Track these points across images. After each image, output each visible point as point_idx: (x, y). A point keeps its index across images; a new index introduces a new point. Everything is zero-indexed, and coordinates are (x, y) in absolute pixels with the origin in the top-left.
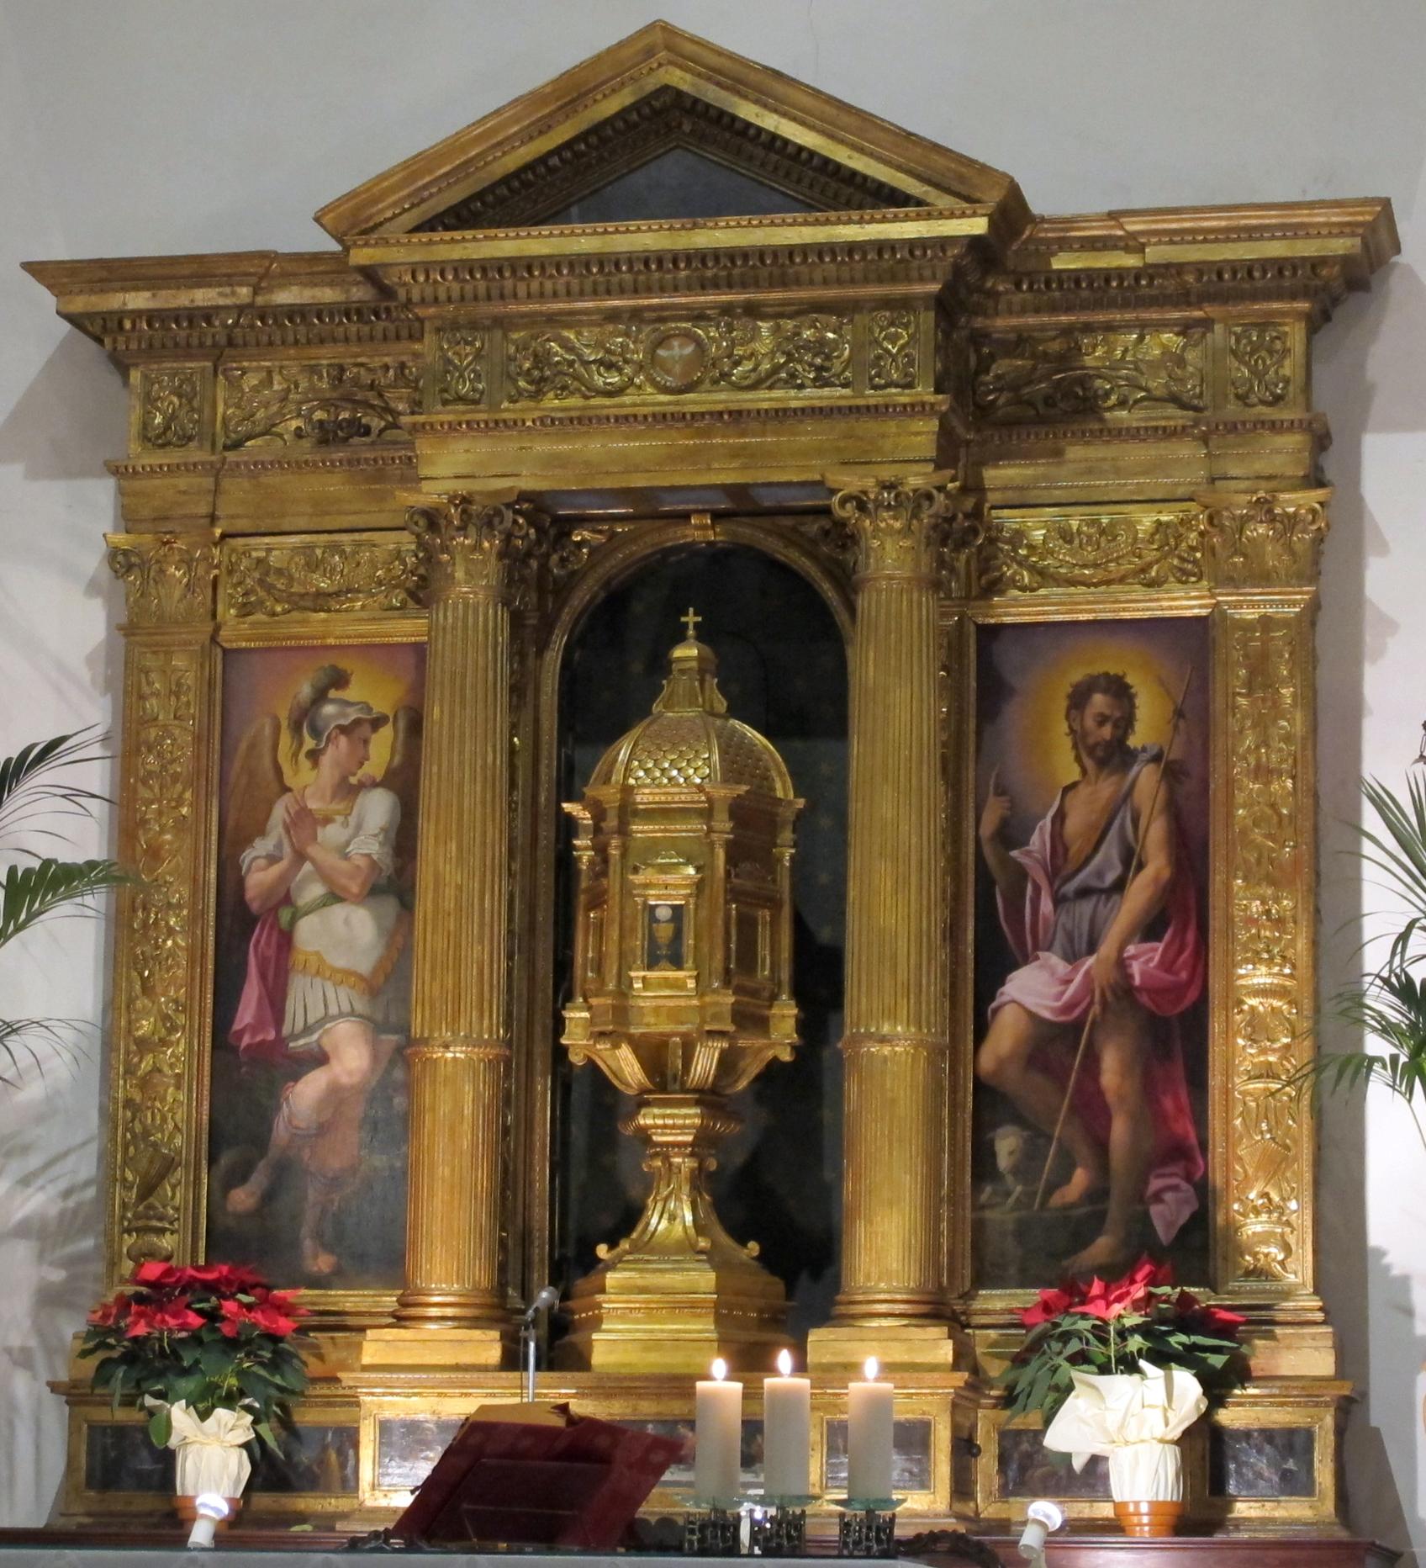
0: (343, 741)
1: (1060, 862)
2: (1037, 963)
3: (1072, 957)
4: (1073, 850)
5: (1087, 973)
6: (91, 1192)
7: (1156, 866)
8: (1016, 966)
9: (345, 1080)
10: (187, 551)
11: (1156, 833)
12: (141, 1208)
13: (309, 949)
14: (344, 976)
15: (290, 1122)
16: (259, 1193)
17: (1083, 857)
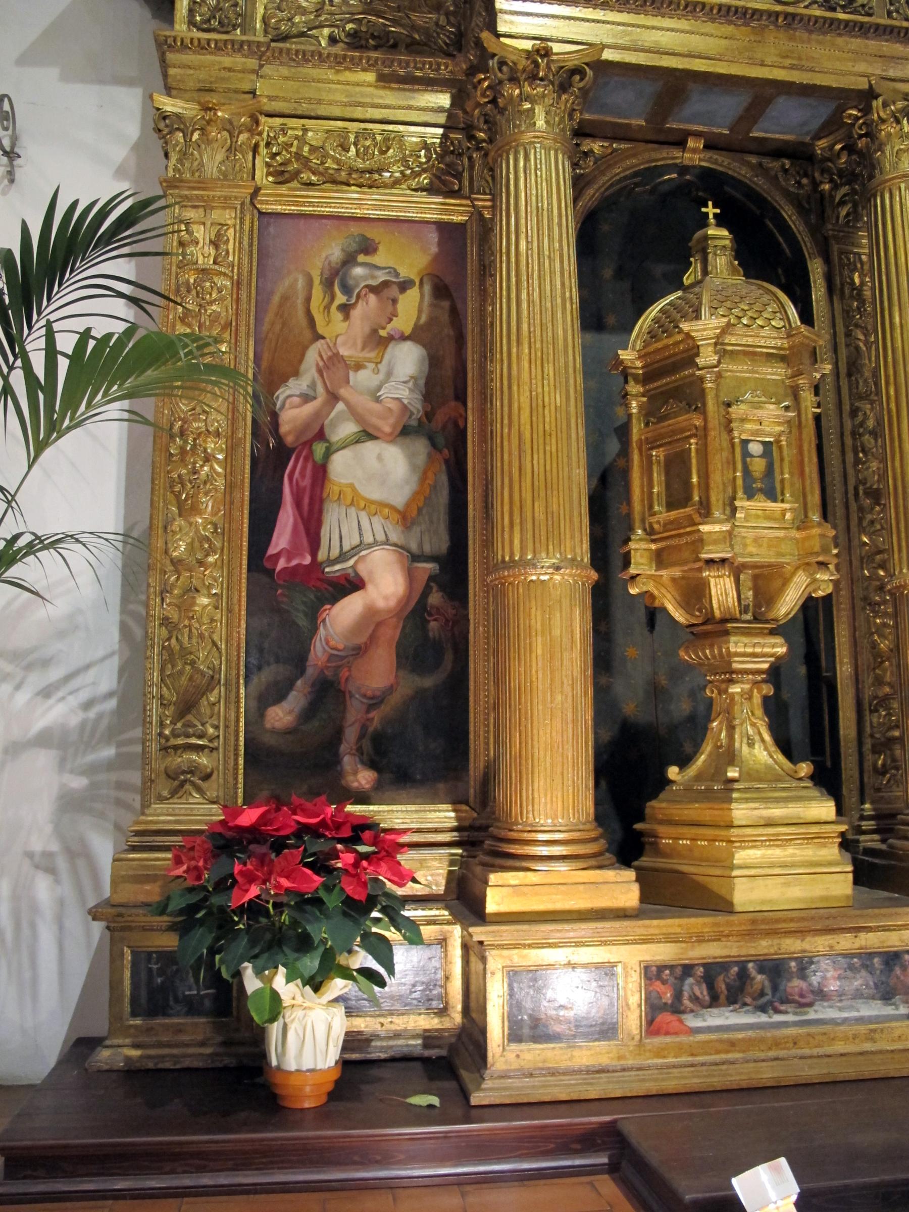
0: (372, 298)
6: (112, 704)
9: (381, 604)
10: (230, 122)
12: (179, 725)
14: (376, 508)
15: (327, 643)
16: (297, 710)
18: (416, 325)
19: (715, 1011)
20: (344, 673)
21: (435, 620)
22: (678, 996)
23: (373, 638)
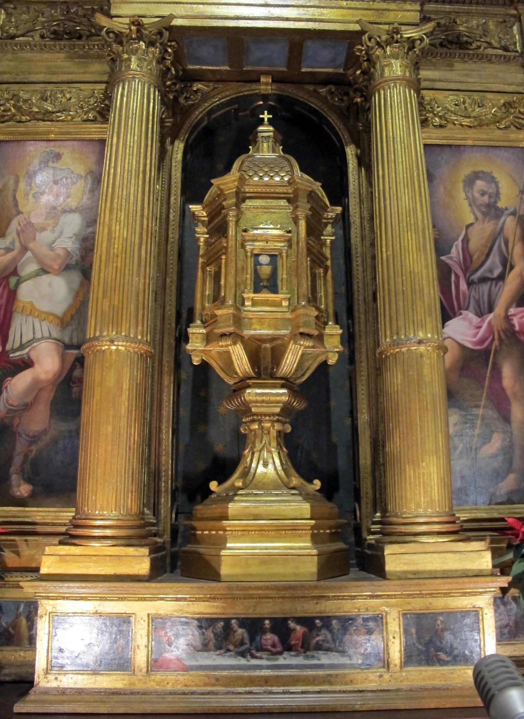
1: (468, 263)
2: (461, 317)
3: (480, 314)
4: (475, 257)
5: (490, 323)
9: (43, 376)
13: (26, 300)
14: (44, 316)
17: (480, 262)
19: (205, 654)
20: (16, 421)
21: (77, 387)
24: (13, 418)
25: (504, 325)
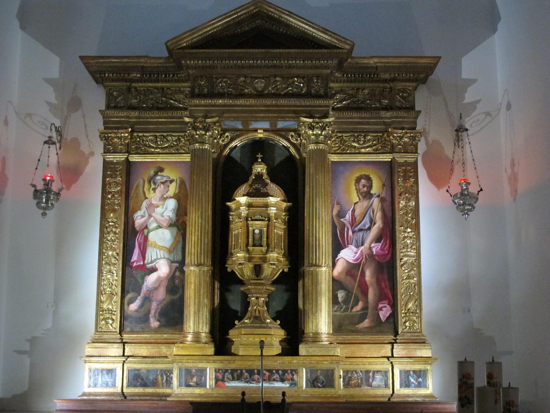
0: (162, 186)
3: (357, 247)
5: (361, 251)
7: (379, 224)
8: (343, 249)
11: (378, 216)
14: (161, 248)
18: (174, 194)
20: (151, 295)
22: (224, 377)
23: (159, 285)
24: (149, 295)
25: (368, 252)
